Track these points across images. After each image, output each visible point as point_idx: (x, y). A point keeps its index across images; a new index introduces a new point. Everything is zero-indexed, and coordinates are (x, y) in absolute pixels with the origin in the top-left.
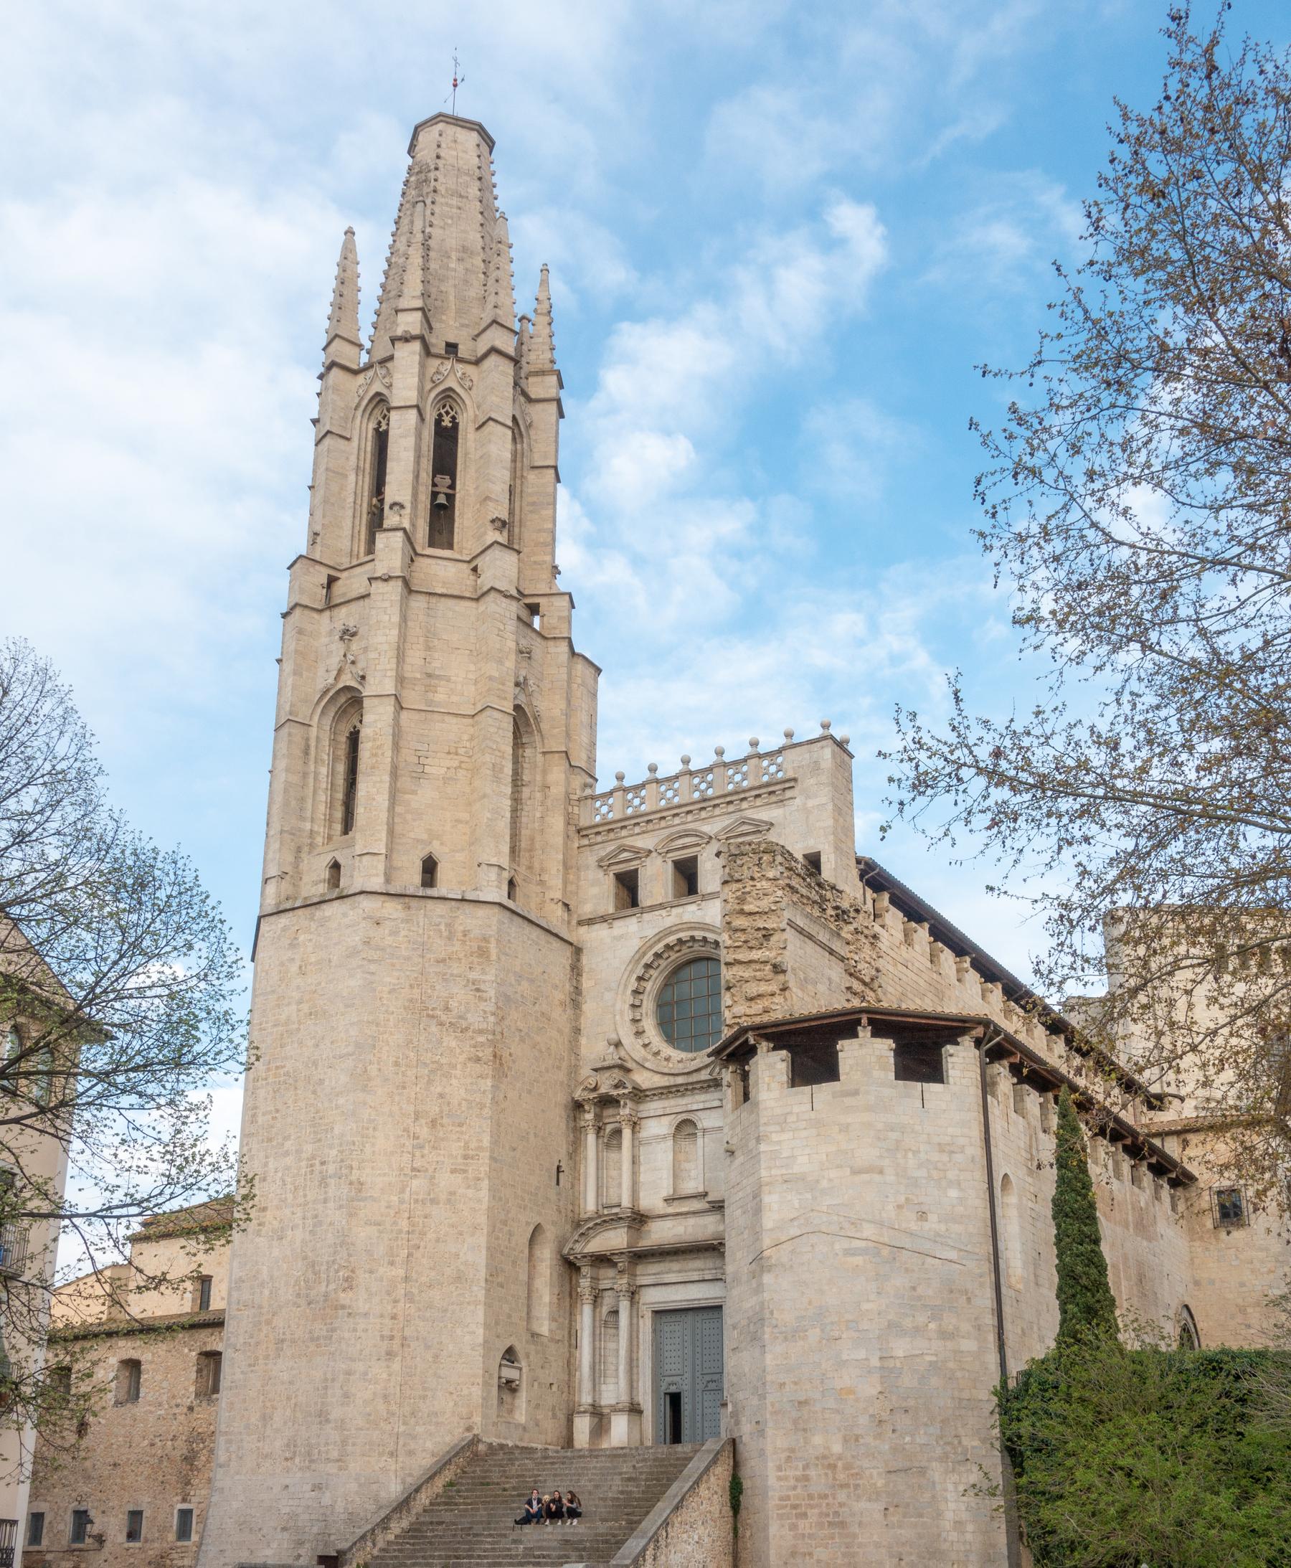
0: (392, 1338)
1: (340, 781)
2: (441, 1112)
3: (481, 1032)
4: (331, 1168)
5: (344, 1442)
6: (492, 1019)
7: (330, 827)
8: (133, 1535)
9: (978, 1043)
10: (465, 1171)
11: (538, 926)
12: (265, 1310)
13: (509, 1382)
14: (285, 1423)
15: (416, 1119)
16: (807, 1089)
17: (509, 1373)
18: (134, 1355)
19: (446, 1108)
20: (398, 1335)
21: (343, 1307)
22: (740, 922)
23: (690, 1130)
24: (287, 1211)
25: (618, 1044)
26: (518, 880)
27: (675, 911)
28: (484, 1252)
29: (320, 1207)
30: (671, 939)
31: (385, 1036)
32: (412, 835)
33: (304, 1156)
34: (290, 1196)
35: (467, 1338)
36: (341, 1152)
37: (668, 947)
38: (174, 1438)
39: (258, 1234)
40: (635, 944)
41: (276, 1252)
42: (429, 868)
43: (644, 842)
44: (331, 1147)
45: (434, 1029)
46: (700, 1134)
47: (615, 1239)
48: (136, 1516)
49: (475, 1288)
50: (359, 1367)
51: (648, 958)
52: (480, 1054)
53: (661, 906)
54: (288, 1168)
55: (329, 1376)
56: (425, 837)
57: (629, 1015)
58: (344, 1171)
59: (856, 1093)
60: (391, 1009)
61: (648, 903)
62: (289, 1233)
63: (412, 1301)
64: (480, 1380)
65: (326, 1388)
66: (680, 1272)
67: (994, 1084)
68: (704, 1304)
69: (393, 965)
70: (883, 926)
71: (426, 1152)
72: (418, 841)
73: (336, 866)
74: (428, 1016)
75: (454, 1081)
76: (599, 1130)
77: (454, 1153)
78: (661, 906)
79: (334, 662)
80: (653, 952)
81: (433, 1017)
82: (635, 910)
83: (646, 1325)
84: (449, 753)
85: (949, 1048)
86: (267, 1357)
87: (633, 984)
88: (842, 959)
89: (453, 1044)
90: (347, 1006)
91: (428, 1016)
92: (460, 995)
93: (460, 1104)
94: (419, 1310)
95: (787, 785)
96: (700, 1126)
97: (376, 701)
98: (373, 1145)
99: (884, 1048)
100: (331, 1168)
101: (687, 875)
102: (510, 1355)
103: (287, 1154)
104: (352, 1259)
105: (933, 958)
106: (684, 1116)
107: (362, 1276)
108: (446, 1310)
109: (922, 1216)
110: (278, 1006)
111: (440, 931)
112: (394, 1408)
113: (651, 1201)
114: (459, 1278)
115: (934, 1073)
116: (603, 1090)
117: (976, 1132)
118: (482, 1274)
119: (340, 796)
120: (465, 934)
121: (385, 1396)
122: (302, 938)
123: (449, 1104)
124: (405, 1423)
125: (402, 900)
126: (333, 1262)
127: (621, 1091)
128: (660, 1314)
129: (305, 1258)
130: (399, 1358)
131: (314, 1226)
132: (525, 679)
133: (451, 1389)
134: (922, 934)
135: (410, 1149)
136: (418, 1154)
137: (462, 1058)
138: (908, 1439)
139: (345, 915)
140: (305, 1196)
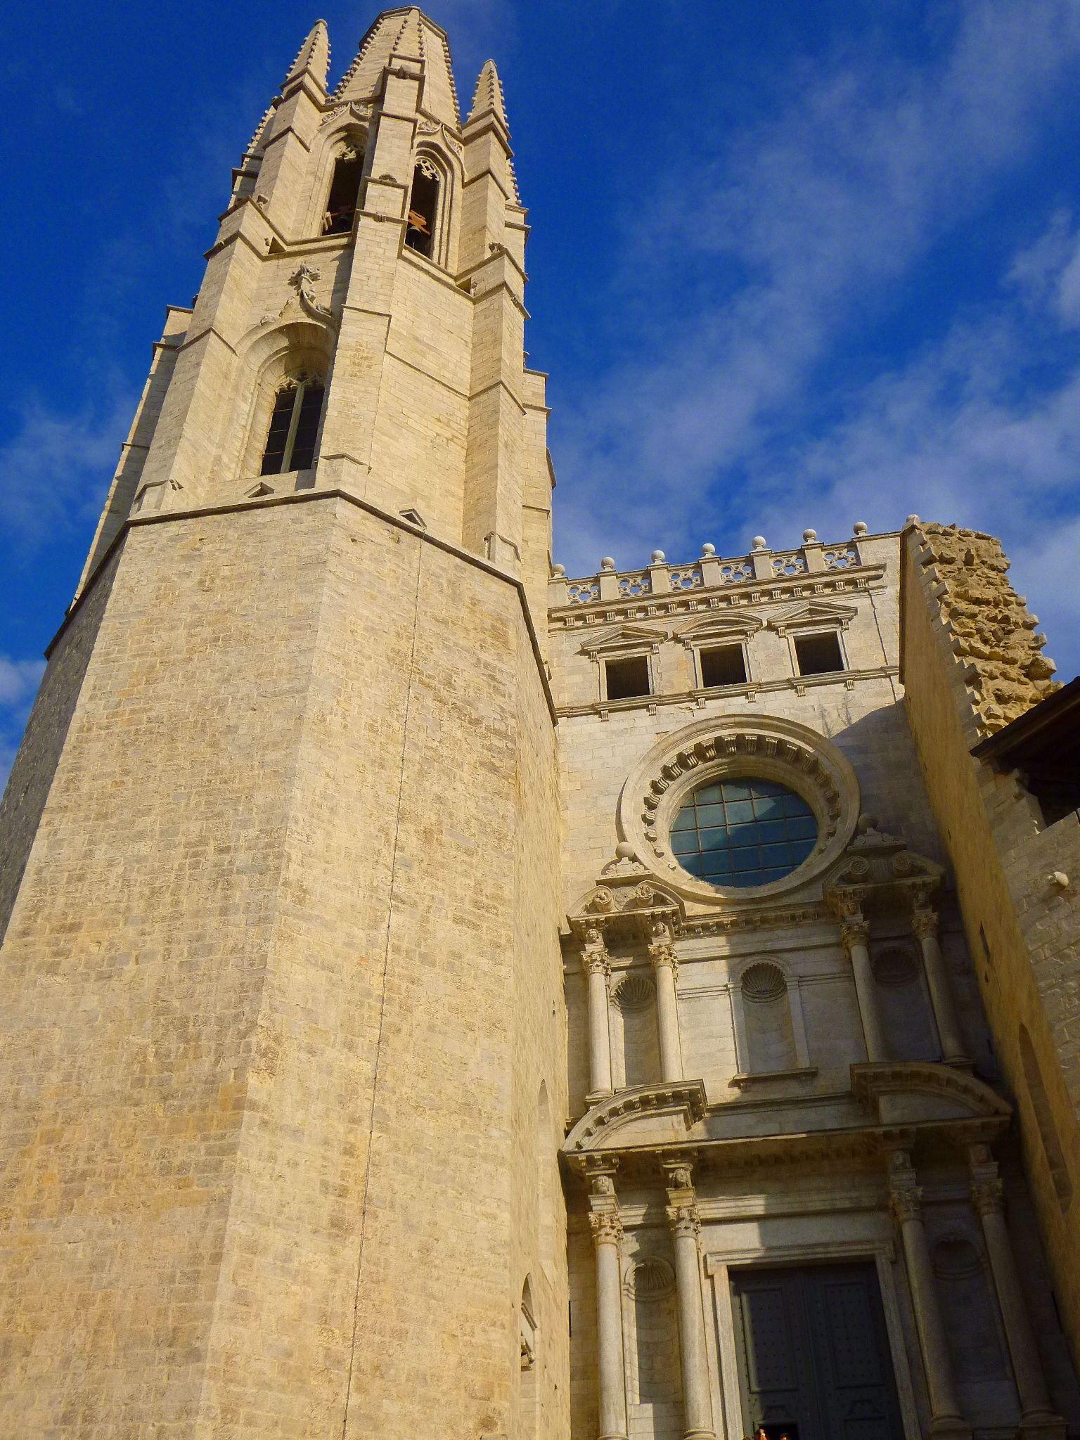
0: (343, 1192)
2: (440, 823)
3: (497, 732)
4: (242, 858)
5: (229, 1412)
6: (512, 722)
7: (242, 470)
10: (476, 927)
12: (45, 1114)
14: (66, 1362)
15: (401, 818)
19: (446, 820)
20: (355, 1189)
21: (253, 1106)
22: (962, 606)
24: (131, 932)
25: (634, 859)
28: (508, 1070)
29: (213, 922)
30: (707, 738)
31: (357, 685)
32: (389, 480)
33: (181, 839)
34: (139, 907)
35: (483, 1223)
36: (269, 833)
39: (52, 970)
40: (650, 740)
41: (91, 1002)
44: (245, 824)
45: (429, 702)
46: (791, 984)
49: (495, 1133)
50: (276, 1239)
52: (498, 764)
53: (692, 697)
54: (140, 860)
55: (206, 1249)
56: (407, 490)
58: (271, 862)
60: (367, 651)
63: (384, 1129)
64: (506, 1318)
65: (195, 1277)
68: (835, 1252)
69: (373, 597)
72: (397, 490)
74: (421, 682)
77: (459, 891)
78: (692, 697)
80: (676, 752)
81: (428, 686)
84: (439, 420)
86: (35, 1212)
90: (292, 628)
91: (421, 682)
92: (468, 678)
93: (468, 822)
94: (396, 1147)
95: (873, 573)
96: (787, 971)
97: (356, 314)
98: (328, 834)
100: (242, 858)
101: (724, 669)
103: (141, 836)
104: (277, 1016)
106: (758, 960)
107: (292, 1055)
108: (444, 1162)
110: (150, 631)
111: (441, 585)
112: (339, 1347)
114: (467, 1107)
118: (507, 1109)
121: (324, 1318)
122: (206, 549)
123: (451, 815)
124: (361, 1389)
125: (389, 526)
126: (237, 1018)
127: (658, 910)
129: (166, 1011)
130: (358, 1240)
131: (193, 953)
133: (454, 1326)
135: (389, 861)
136: (401, 873)
137: (472, 758)
140: (176, 903)
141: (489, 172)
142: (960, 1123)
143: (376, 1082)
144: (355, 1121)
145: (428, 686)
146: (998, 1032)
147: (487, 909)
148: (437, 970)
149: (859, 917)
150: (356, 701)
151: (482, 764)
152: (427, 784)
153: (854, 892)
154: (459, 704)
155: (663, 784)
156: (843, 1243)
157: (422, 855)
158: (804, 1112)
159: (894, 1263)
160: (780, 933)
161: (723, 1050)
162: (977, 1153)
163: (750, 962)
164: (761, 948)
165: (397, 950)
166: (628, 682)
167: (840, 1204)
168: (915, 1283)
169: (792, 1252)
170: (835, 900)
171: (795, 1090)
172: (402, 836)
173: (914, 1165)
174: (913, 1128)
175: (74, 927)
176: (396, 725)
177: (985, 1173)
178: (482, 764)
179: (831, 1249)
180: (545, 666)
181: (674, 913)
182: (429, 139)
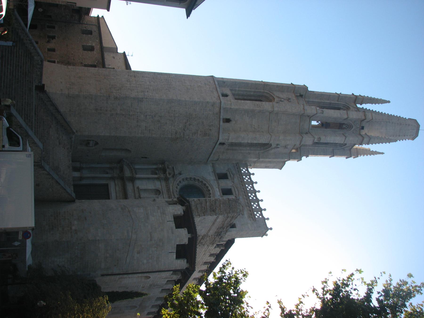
0: (101, 110)
1: (249, 98)
3: (184, 134)
4: (146, 94)
6: (187, 137)
8: (49, 50)
9: (187, 269)
11: (213, 151)
13: (89, 143)
16: (173, 220)
17: (91, 143)
18: (95, 50)
25: (180, 174)
26: (225, 146)
27: (217, 189)
30: (210, 188)
37: (207, 187)
38: (74, 59)
39: (128, 76)
42: (228, 121)
43: (236, 180)
46: (157, 196)
47: (127, 173)
48: (53, 50)
51: (204, 182)
57: (188, 177)
59: (173, 233)
61: (220, 182)
62: (129, 83)
67: (175, 274)
70: (215, 247)
73: (226, 96)
75: (170, 127)
76: (156, 169)
78: (219, 185)
79: (281, 96)
83: (104, 182)
85: (186, 261)
87: (197, 178)
88: (207, 234)
96: (159, 196)
99: (185, 241)
101: (227, 192)
102: (97, 143)
103: (150, 83)
105: (206, 263)
106: (161, 192)
109: (139, 253)
113: (138, 183)
115: (178, 257)
116: (168, 170)
117: (162, 268)
119: (245, 98)
120: (210, 130)
122: (208, 86)
128: (107, 185)
132: (278, 147)
134: (212, 259)
138: (76, 247)
139: (214, 97)
141: (346, 137)
143: (117, 114)
144: (111, 111)
147: (150, 132)
165: (138, 116)
175: (135, 77)
182: (353, 125)
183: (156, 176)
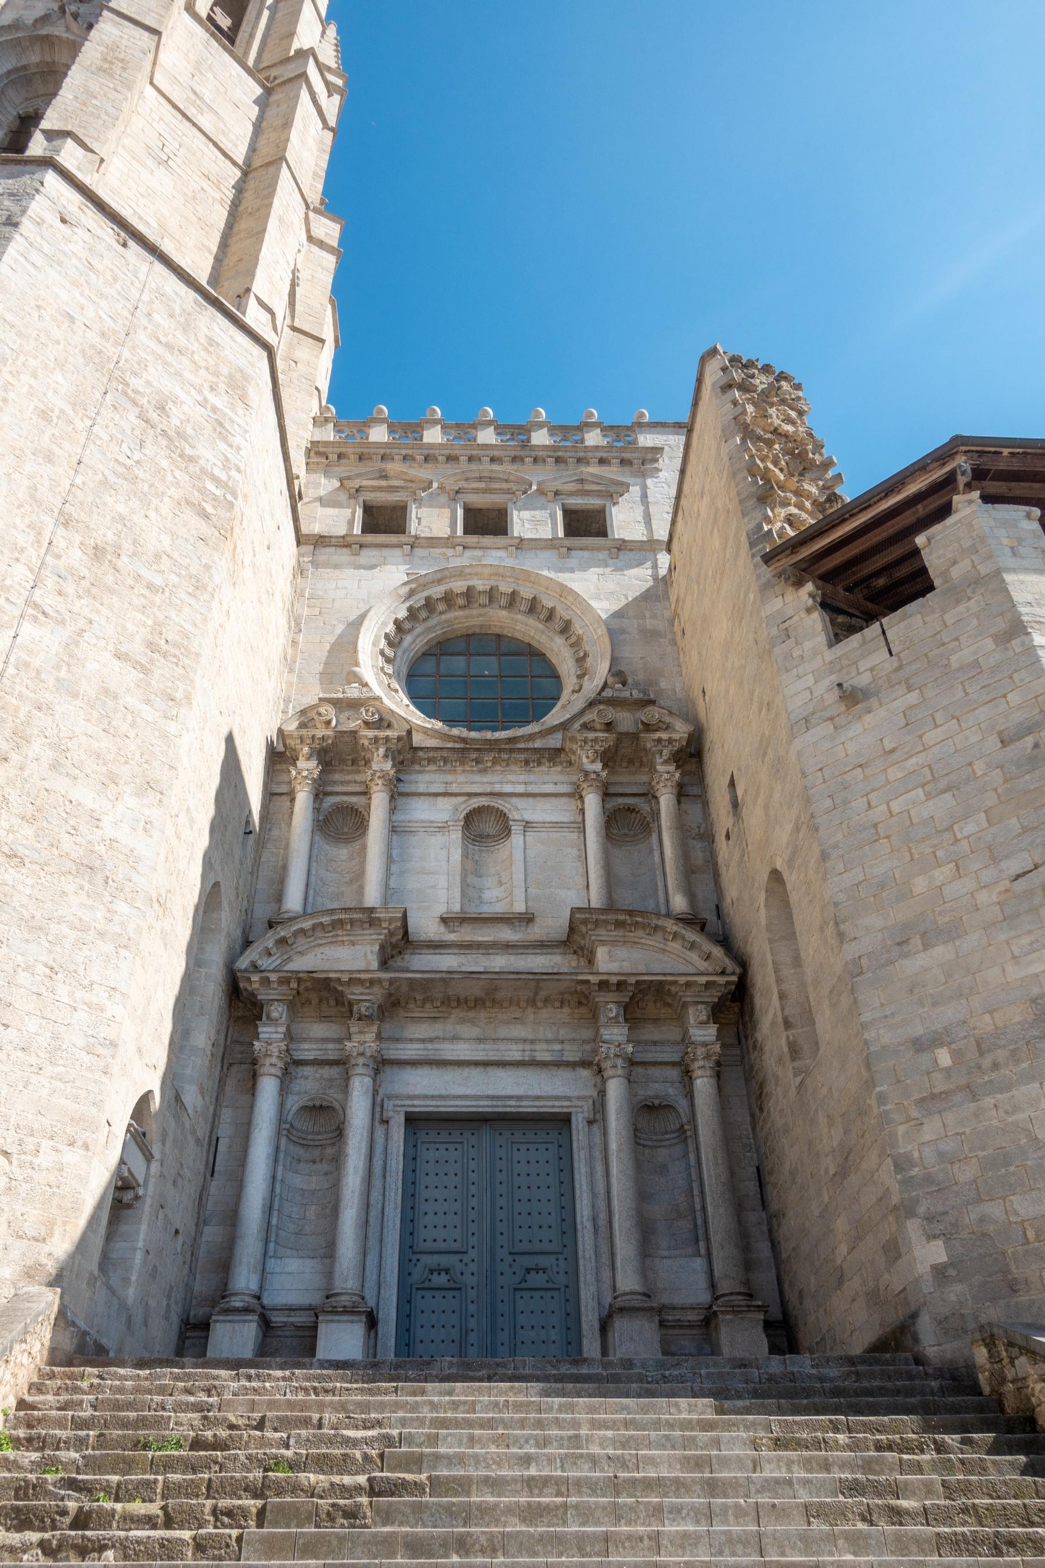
10: (145, 671)
23: (490, 827)
27: (469, 553)
30: (459, 586)
35: (82, 1015)
45: (132, 417)
46: (516, 829)
52: (209, 509)
53: (448, 542)
66: (480, 1040)
68: (527, 1107)
71: (70, 588)
76: (319, 794)
80: (426, 594)
81: (135, 403)
82: (402, 538)
89: (165, 463)
91: (125, 394)
93: (157, 557)
96: (514, 815)
123: (135, 542)
127: (382, 734)
135: (36, 563)
136: (50, 582)
142: (682, 980)
145: (135, 403)
146: (732, 892)
148: (78, 703)
149: (598, 766)
150: (26, 378)
151: (188, 502)
152: (110, 500)
153: (595, 740)
154: (172, 433)
155: (407, 626)
156: (538, 1098)
157: (85, 572)
158: (513, 958)
159: (590, 1123)
160: (511, 777)
161: (434, 887)
162: (697, 1015)
163: (476, 802)
164: (488, 790)
166: (383, 521)
167: (541, 1056)
168: (613, 1146)
169: (481, 1103)
170: (574, 747)
171: (507, 934)
172: (60, 543)
173: (626, 1020)
174: (632, 980)
176: (80, 425)
177: (704, 1034)
178: (188, 502)
179: (524, 1103)
180: (296, 482)
181: (399, 739)
183: (379, 801)
